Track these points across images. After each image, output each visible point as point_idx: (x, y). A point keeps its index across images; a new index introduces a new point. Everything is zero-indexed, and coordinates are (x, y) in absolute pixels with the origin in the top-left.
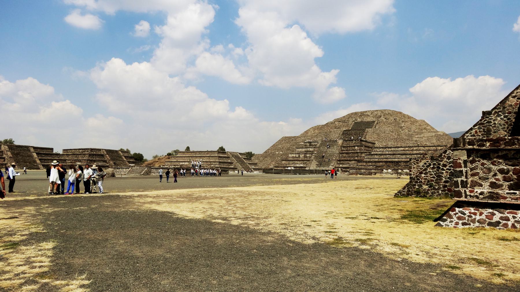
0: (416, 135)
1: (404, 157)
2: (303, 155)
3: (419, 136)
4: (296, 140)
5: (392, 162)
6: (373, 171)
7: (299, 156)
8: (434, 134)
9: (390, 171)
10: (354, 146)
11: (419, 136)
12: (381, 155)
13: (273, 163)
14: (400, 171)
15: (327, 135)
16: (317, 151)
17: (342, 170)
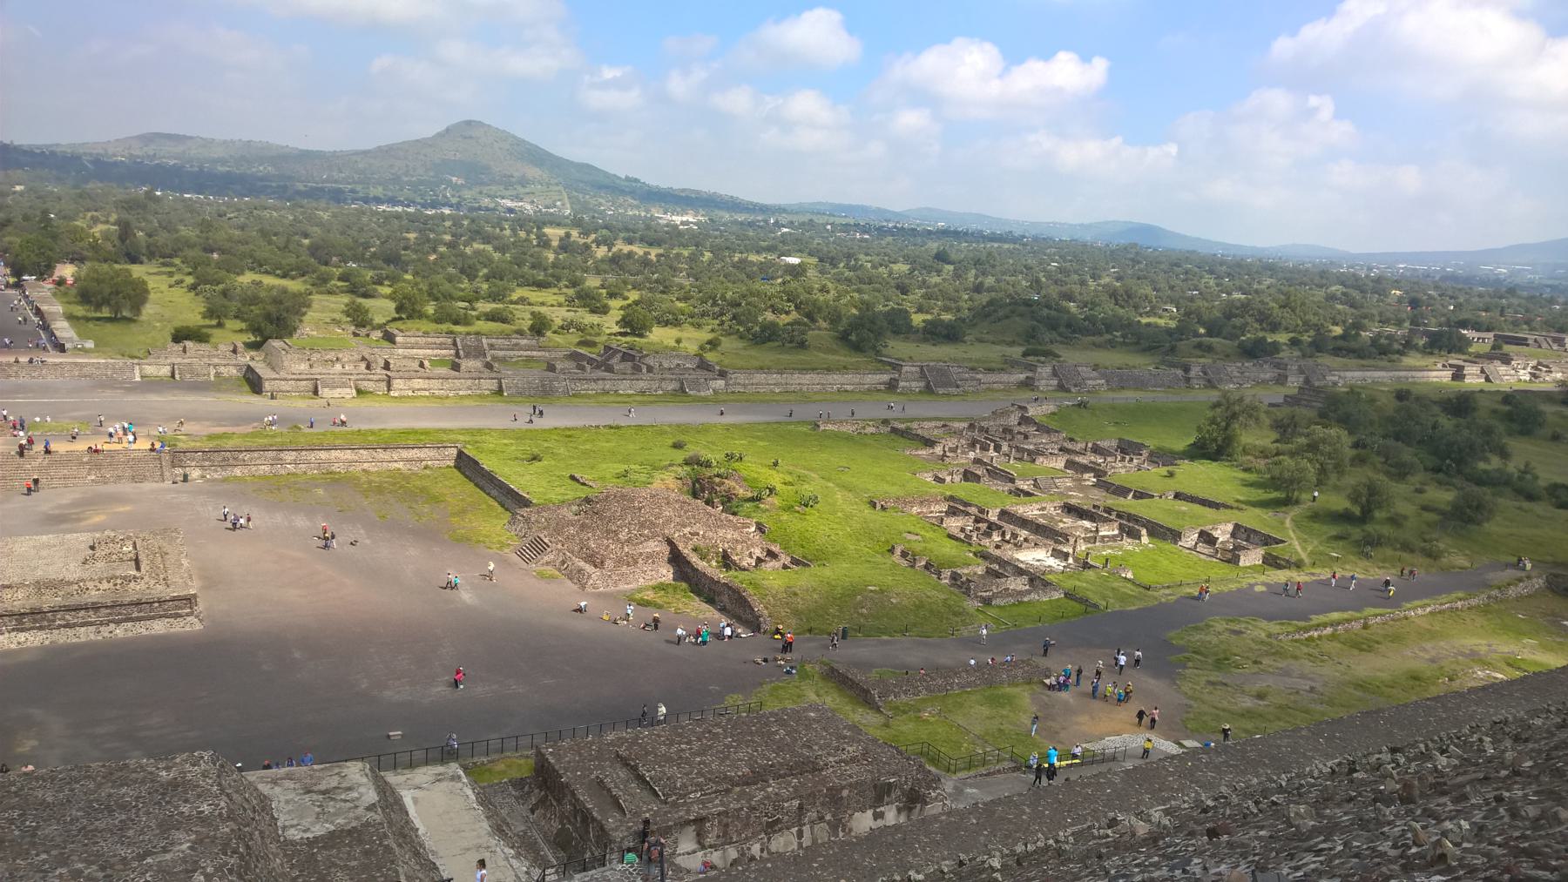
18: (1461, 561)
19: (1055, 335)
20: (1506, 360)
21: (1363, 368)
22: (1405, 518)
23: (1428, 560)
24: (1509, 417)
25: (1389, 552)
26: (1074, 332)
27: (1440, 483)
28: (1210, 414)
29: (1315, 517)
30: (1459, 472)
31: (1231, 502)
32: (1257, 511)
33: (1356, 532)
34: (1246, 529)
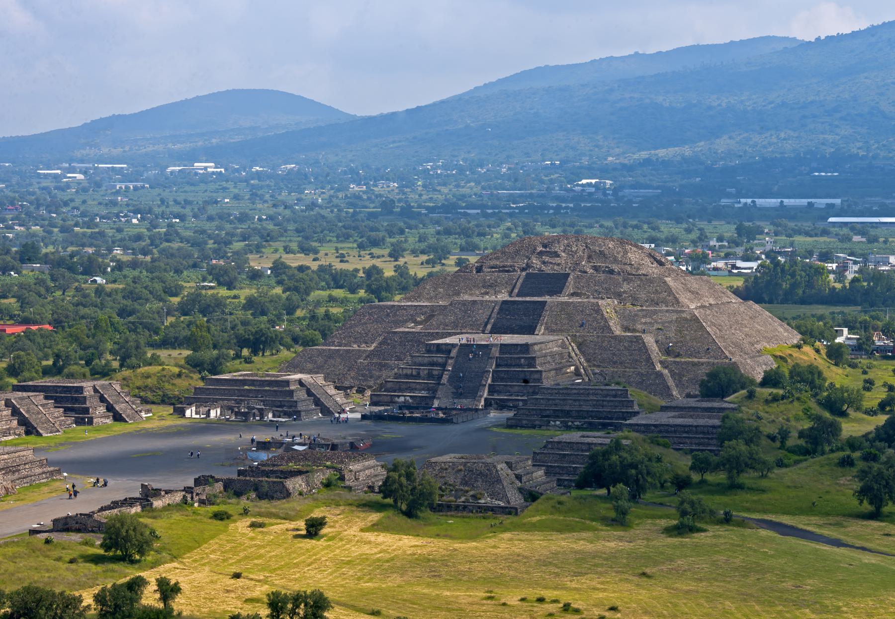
0: (645, 316)
1: (577, 403)
2: (426, 372)
3: (648, 320)
4: (395, 315)
5: (562, 411)
6: (537, 423)
7: (419, 374)
8: (674, 317)
9: (558, 423)
10: (519, 358)
11: (648, 320)
12: (549, 400)
13: (353, 374)
14: (570, 424)
15: (465, 312)
16: (454, 367)
17: (497, 403)
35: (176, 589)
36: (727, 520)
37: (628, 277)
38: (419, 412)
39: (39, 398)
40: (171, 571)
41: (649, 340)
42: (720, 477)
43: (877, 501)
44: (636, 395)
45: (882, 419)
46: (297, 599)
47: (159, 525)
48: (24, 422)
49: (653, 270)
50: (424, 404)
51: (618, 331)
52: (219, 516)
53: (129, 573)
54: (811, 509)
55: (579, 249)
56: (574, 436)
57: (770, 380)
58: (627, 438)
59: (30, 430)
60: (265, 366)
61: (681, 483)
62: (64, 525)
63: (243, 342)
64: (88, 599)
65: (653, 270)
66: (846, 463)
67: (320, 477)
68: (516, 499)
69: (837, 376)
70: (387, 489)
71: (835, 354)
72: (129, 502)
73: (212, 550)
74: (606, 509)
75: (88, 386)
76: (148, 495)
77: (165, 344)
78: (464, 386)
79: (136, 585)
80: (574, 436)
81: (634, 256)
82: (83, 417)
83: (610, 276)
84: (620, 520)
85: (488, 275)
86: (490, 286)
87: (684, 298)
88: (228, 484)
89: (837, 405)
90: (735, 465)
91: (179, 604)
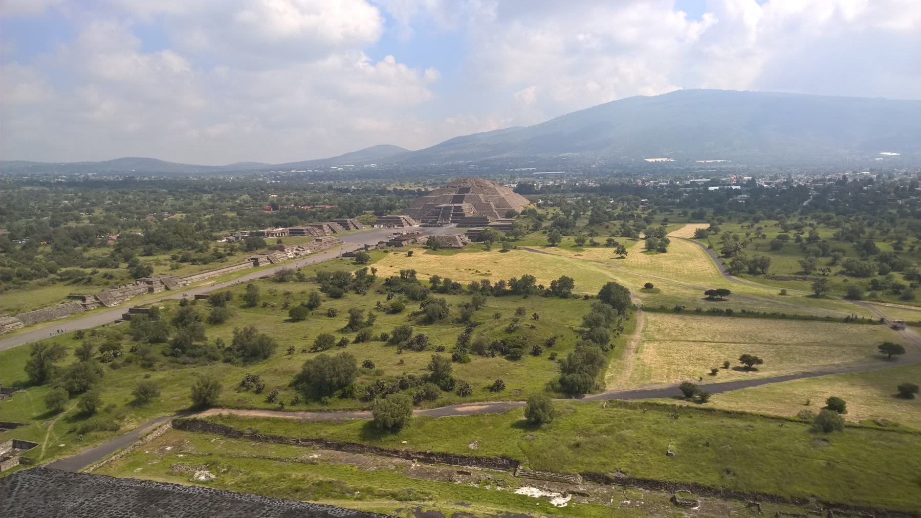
18: (132, 426)
19: (10, 284)
20: (282, 249)
21: (210, 270)
22: (114, 406)
23: (112, 433)
24: (246, 298)
25: (93, 434)
26: (24, 279)
27: (172, 362)
28: (30, 359)
29: (68, 420)
30: (183, 353)
31: (24, 421)
32: (37, 422)
33: (80, 425)
34: (19, 442)
35: (376, 270)
36: (515, 248)
37: (486, 188)
38: (434, 224)
39: (336, 224)
40: (374, 266)
41: (492, 204)
42: (512, 238)
43: (553, 242)
44: (489, 218)
45: (552, 222)
46: (408, 271)
47: (370, 254)
48: (332, 230)
49: (492, 186)
50: (435, 222)
51: (483, 201)
52: (386, 252)
53: (363, 267)
54: (536, 245)
55: (473, 181)
56: (475, 229)
57: (523, 213)
58: (489, 229)
59: (334, 232)
60: (393, 215)
61: (503, 239)
62: (346, 255)
63: (388, 208)
64: (353, 274)
65: (492, 186)
66: (544, 233)
67: (411, 241)
68: (461, 245)
69: (540, 211)
70: (428, 243)
71: (539, 206)
72: (362, 249)
73: (385, 260)
74: (484, 246)
75: (348, 220)
76: (367, 247)
77: (368, 209)
78: (445, 217)
79: (365, 270)
80: (475, 229)
81: (487, 182)
82: (348, 228)
83: (481, 188)
84: (488, 249)
85: (450, 188)
86: (450, 191)
87: (500, 193)
88: (387, 243)
89: (541, 218)
90: (516, 234)
91: (377, 274)
